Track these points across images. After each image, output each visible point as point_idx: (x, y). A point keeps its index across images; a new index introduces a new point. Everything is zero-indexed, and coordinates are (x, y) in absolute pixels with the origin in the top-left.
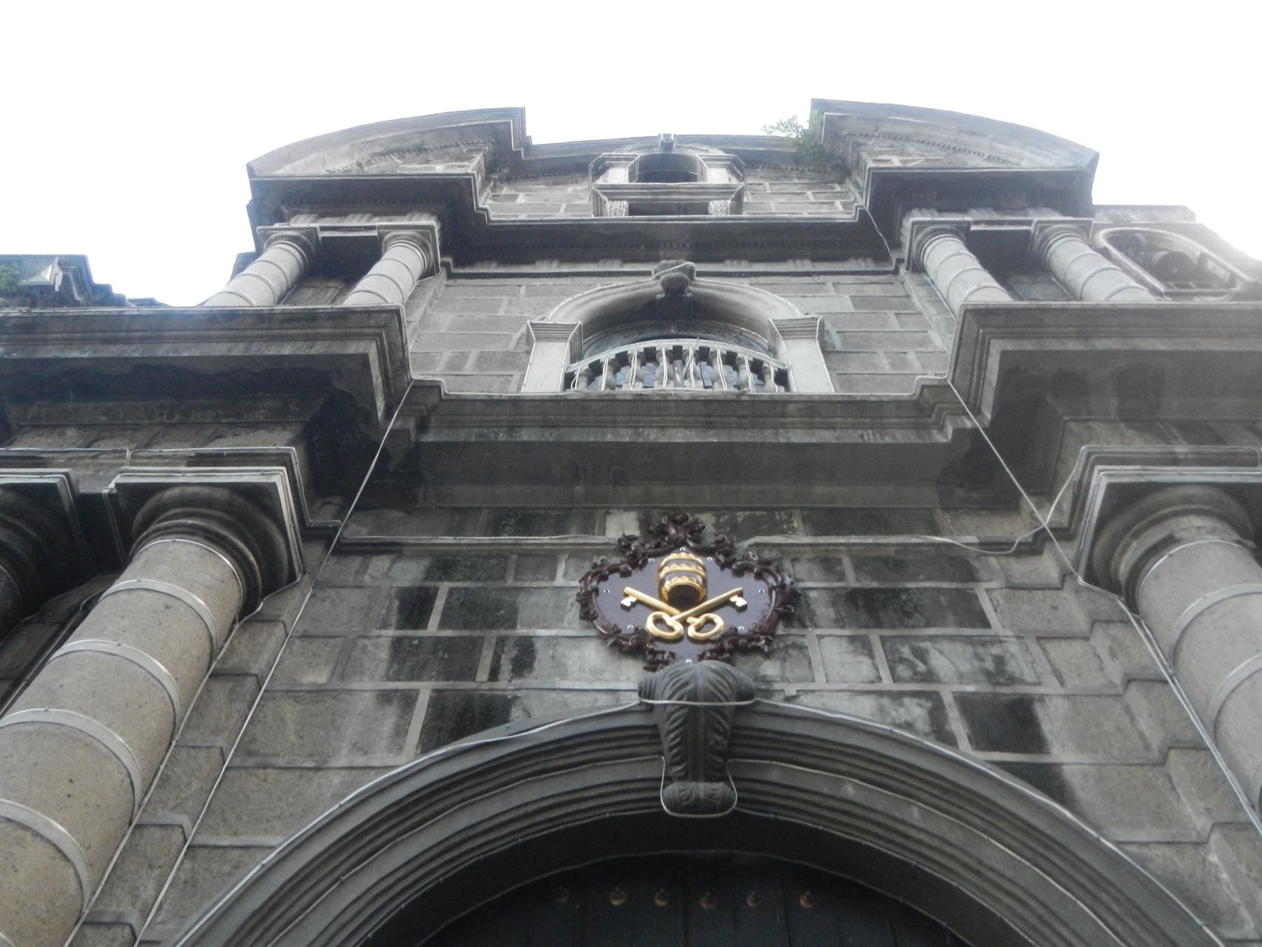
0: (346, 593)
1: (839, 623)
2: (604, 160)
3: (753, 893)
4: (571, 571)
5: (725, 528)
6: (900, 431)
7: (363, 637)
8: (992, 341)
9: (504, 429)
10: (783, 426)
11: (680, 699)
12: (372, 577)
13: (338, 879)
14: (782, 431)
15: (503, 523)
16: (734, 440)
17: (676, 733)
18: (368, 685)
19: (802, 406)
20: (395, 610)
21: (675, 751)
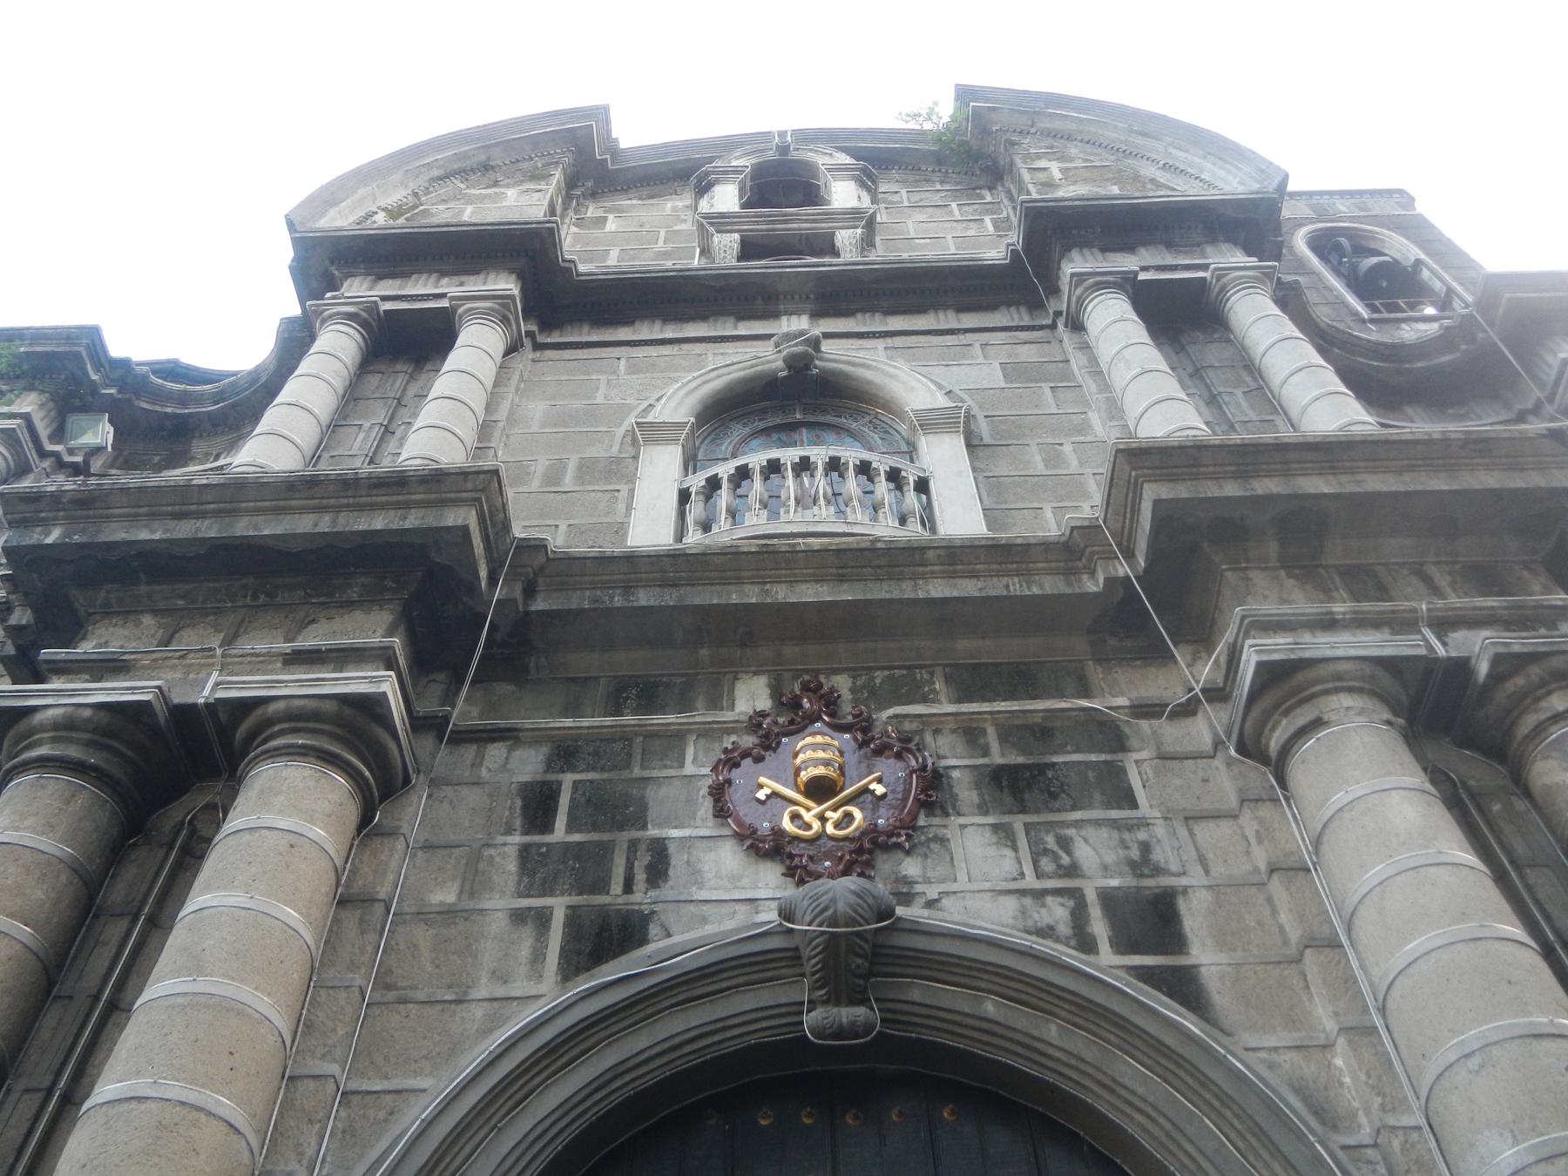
0: (465, 791)
1: (983, 809)
2: (707, 174)
3: (898, 1108)
4: (701, 754)
5: (862, 693)
6: (1049, 577)
7: (489, 846)
8: (1145, 485)
9: (618, 591)
10: (923, 576)
11: (820, 925)
12: (490, 770)
13: (495, 1126)
14: (921, 582)
15: (624, 695)
16: (869, 597)
17: (817, 959)
18: (500, 902)
19: (942, 552)
20: (518, 811)
21: (817, 976)
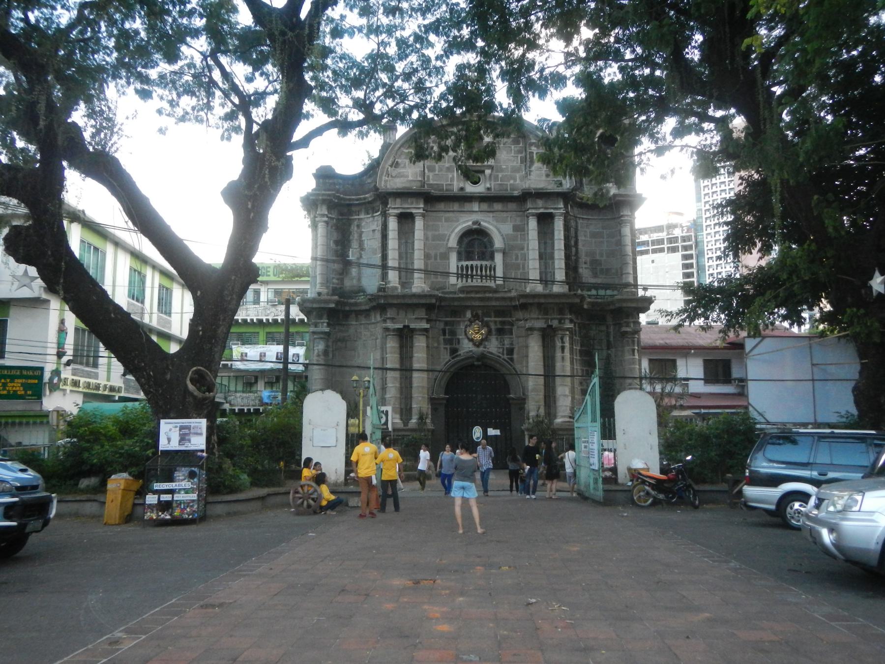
18: (442, 346)
